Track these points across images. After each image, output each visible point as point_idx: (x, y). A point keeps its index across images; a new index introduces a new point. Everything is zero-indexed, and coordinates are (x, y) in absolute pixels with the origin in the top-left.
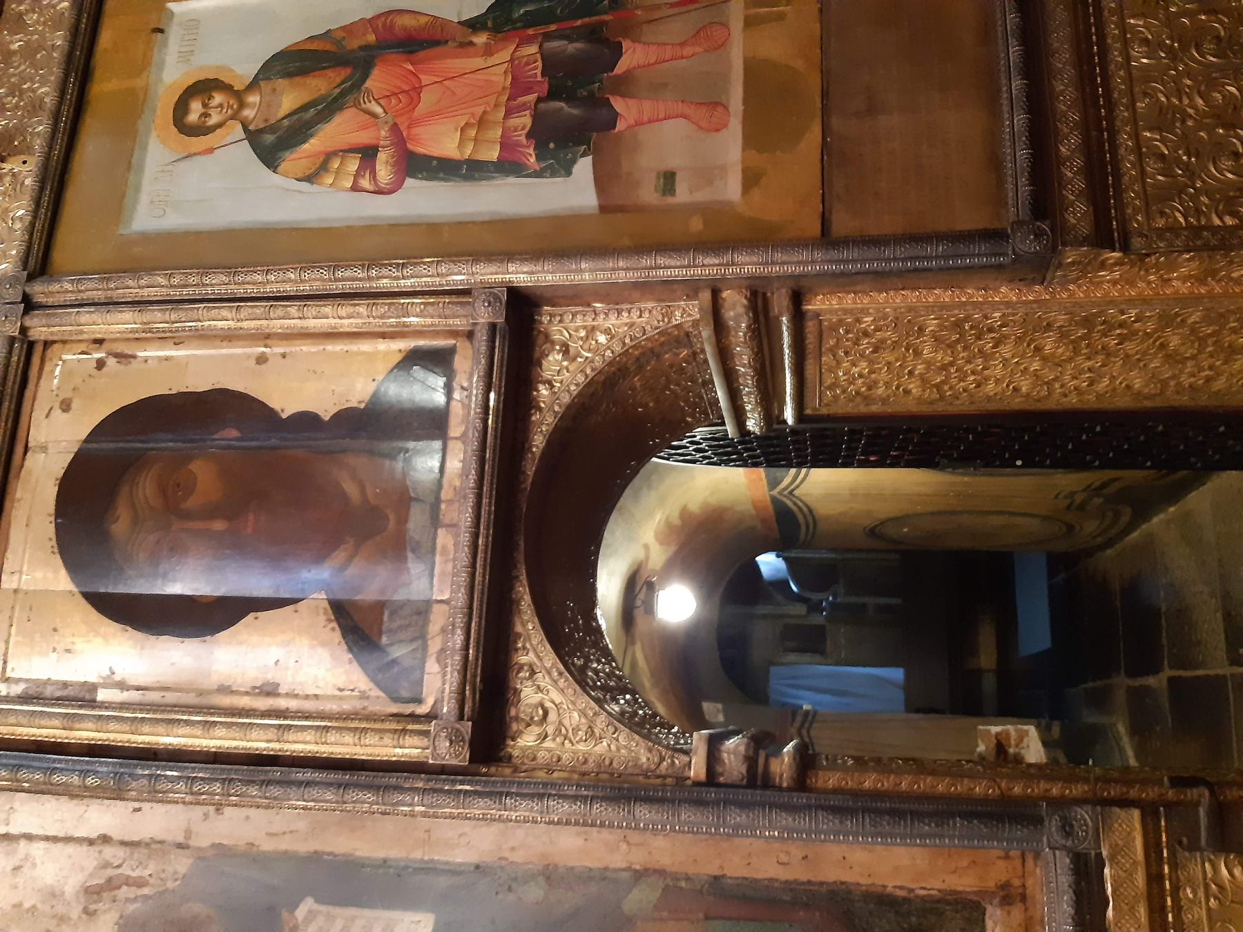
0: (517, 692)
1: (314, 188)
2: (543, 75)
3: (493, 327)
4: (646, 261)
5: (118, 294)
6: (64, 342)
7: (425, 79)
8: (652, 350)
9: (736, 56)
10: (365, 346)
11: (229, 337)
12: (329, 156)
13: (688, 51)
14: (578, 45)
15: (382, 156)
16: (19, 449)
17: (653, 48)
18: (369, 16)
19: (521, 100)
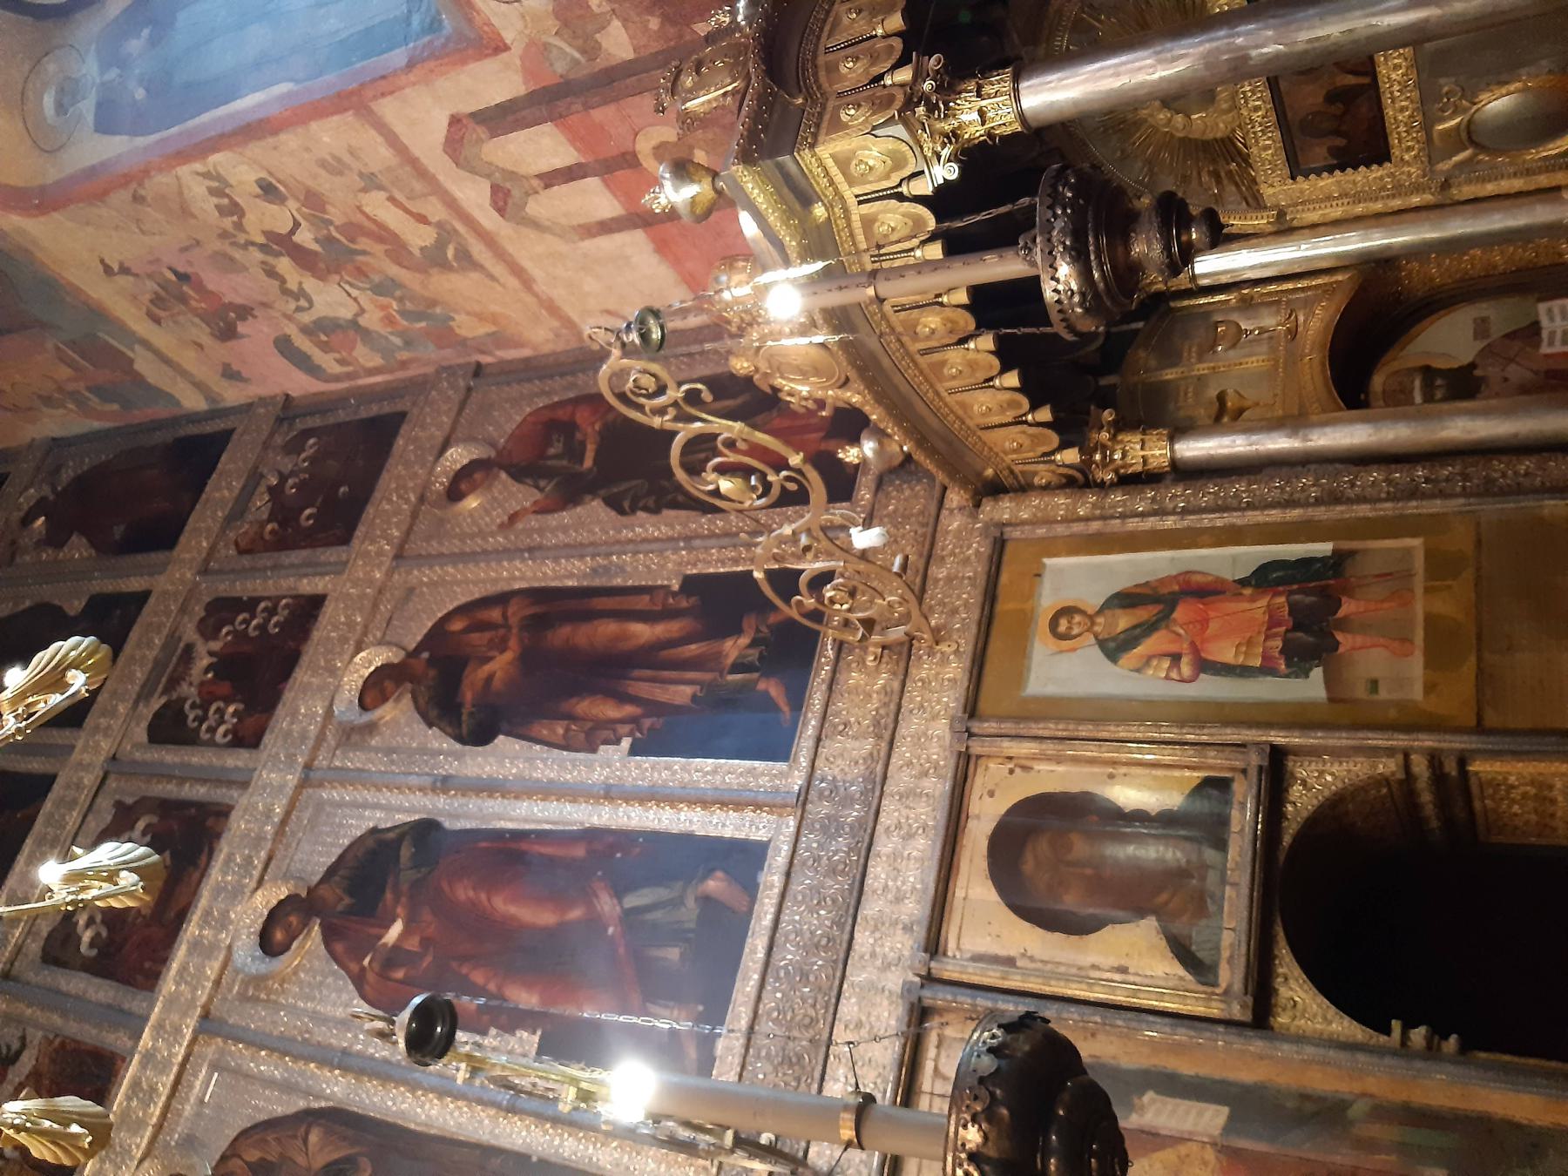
0: (1276, 991)
1: (1141, 676)
2: (1290, 614)
3: (1261, 767)
4: (1360, 735)
5: (1022, 732)
6: (989, 757)
7: (1212, 614)
8: (1362, 788)
9: (1419, 609)
10: (1177, 773)
11: (1092, 761)
12: (1149, 658)
13: (1386, 605)
14: (1313, 599)
15: (1185, 660)
16: (963, 816)
17: (1362, 603)
18: (1174, 573)
19: (1275, 630)
